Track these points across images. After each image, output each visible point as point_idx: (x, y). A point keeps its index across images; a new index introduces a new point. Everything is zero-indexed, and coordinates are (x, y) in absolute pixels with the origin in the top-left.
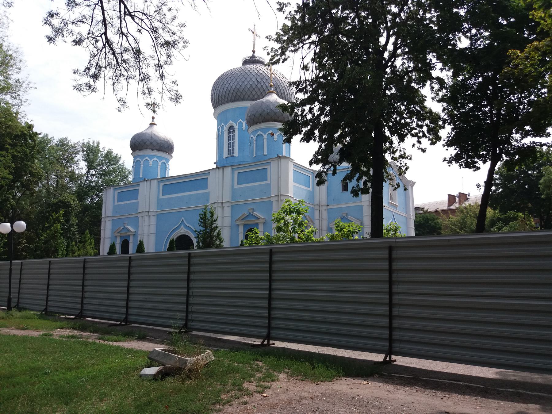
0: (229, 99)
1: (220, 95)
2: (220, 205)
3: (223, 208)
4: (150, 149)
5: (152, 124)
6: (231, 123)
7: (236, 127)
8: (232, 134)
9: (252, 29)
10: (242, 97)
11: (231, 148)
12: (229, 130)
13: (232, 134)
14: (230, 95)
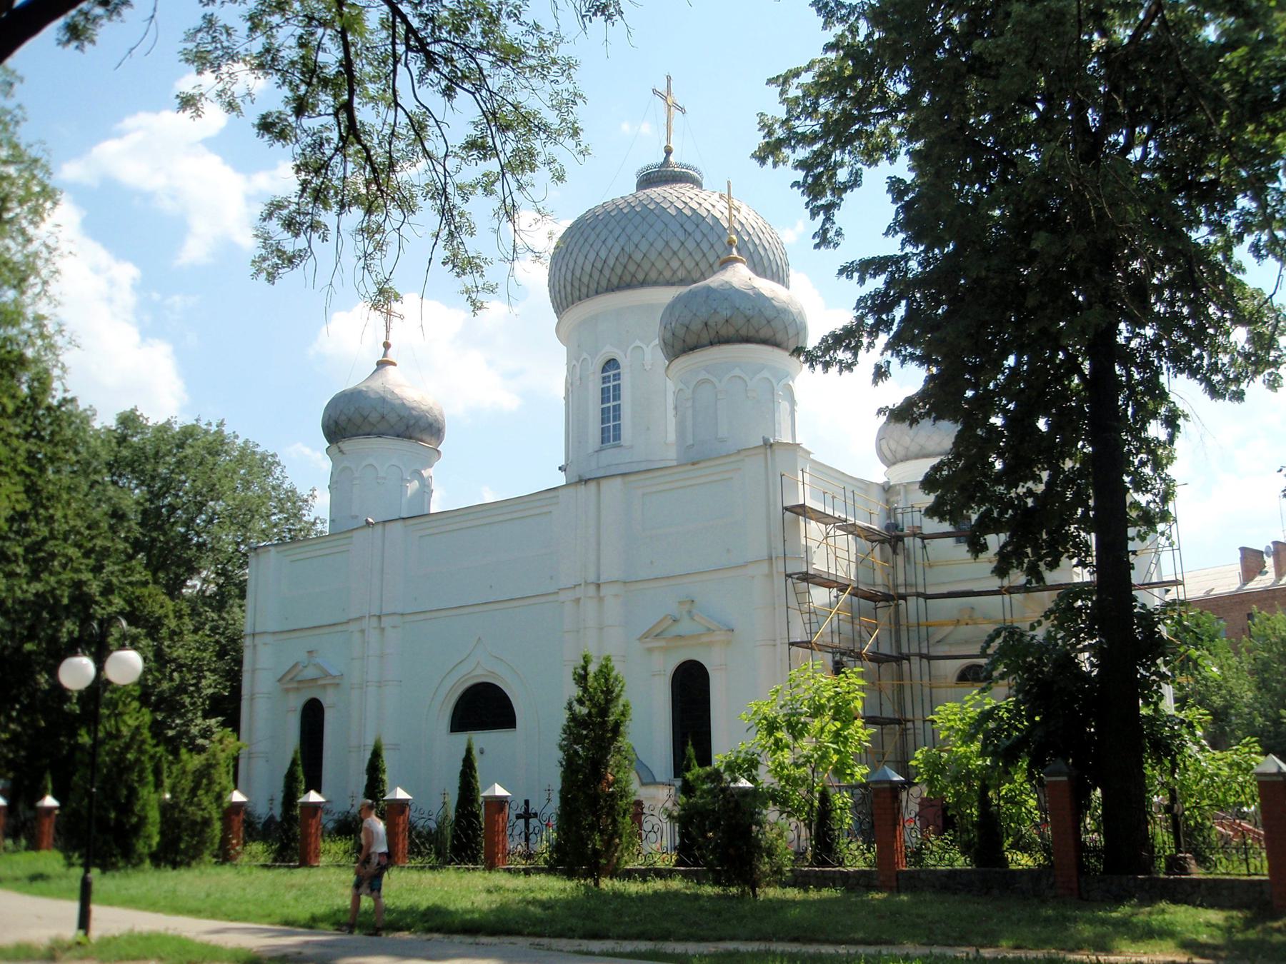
0: (604, 283)
1: (578, 274)
2: (592, 590)
3: (601, 600)
5: (382, 364)
7: (624, 362)
9: (662, 88)
10: (640, 276)
11: (611, 424)
12: (604, 370)
13: (611, 384)
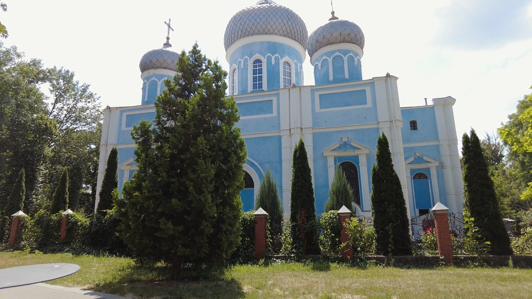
5: (167, 45)
6: (257, 56)
8: (258, 68)
12: (254, 63)
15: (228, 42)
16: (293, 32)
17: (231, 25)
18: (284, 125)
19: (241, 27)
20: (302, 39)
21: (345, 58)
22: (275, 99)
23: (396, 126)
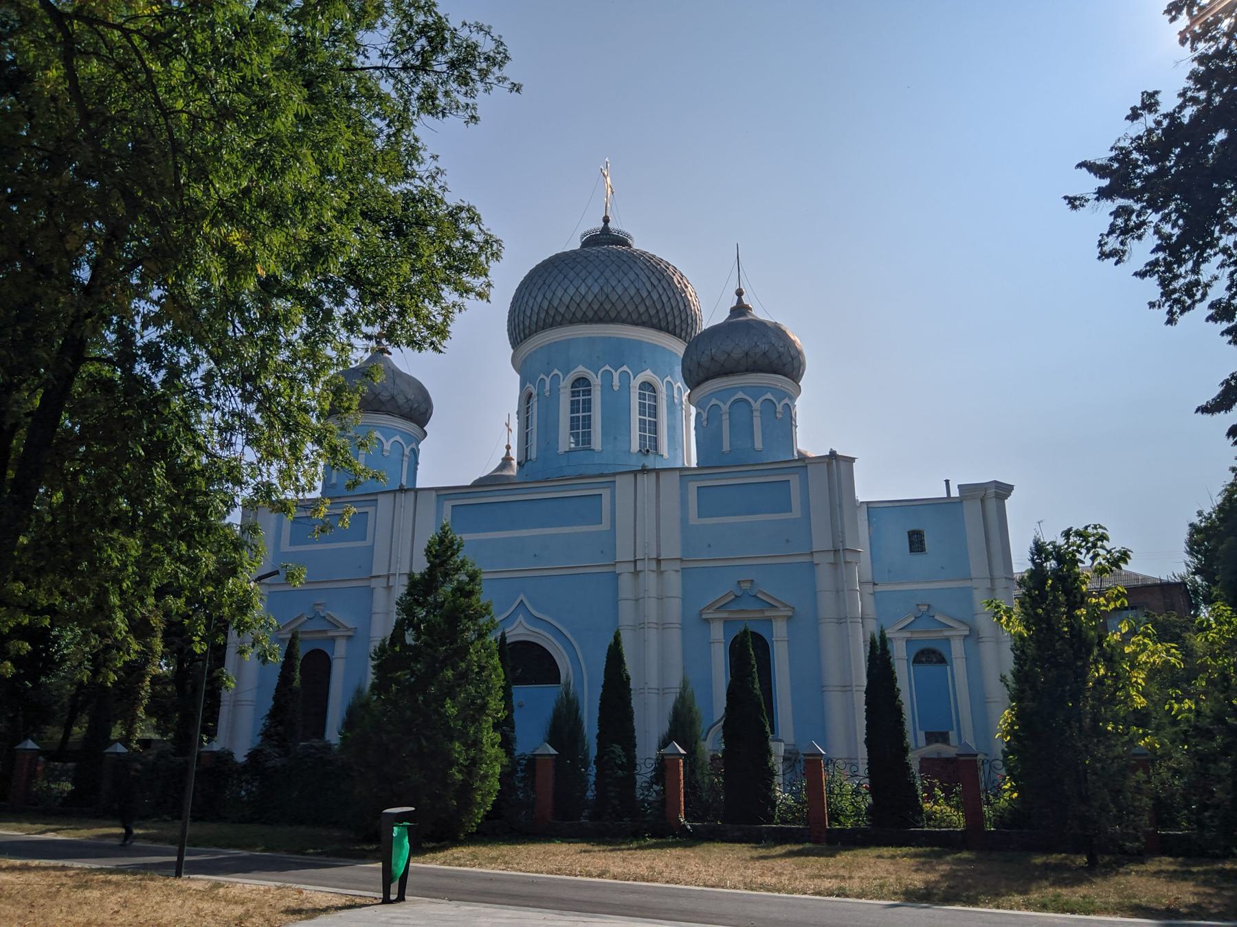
0: (579, 315)
2: (653, 565)
3: (660, 573)
4: (388, 413)
6: (581, 370)
7: (596, 381)
8: (581, 398)
10: (613, 314)
13: (581, 398)
14: (584, 306)
15: (517, 331)
16: (662, 315)
17: (522, 294)
18: (624, 552)
19: (546, 304)
20: (684, 326)
21: (756, 405)
22: (606, 494)
23: (846, 563)
